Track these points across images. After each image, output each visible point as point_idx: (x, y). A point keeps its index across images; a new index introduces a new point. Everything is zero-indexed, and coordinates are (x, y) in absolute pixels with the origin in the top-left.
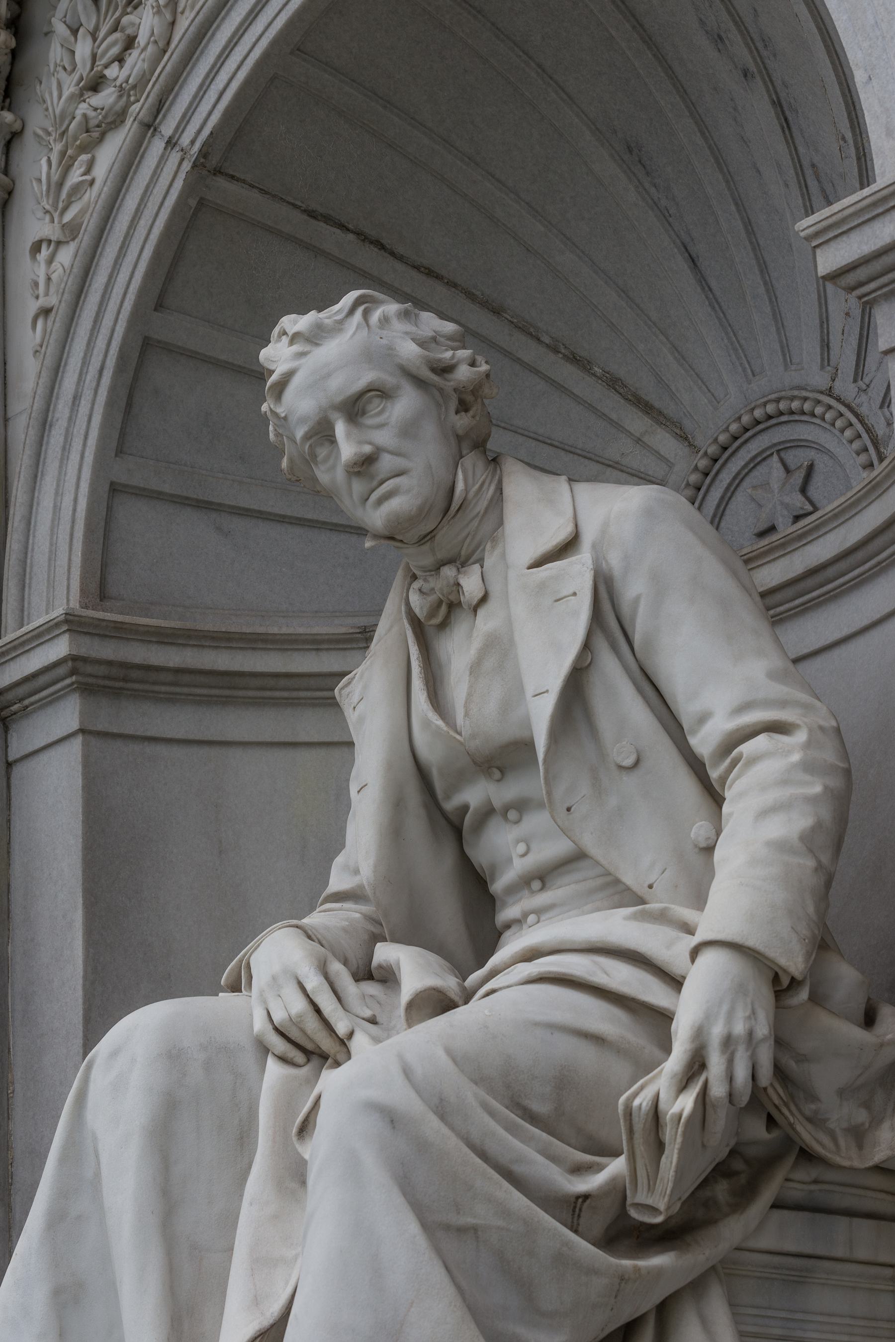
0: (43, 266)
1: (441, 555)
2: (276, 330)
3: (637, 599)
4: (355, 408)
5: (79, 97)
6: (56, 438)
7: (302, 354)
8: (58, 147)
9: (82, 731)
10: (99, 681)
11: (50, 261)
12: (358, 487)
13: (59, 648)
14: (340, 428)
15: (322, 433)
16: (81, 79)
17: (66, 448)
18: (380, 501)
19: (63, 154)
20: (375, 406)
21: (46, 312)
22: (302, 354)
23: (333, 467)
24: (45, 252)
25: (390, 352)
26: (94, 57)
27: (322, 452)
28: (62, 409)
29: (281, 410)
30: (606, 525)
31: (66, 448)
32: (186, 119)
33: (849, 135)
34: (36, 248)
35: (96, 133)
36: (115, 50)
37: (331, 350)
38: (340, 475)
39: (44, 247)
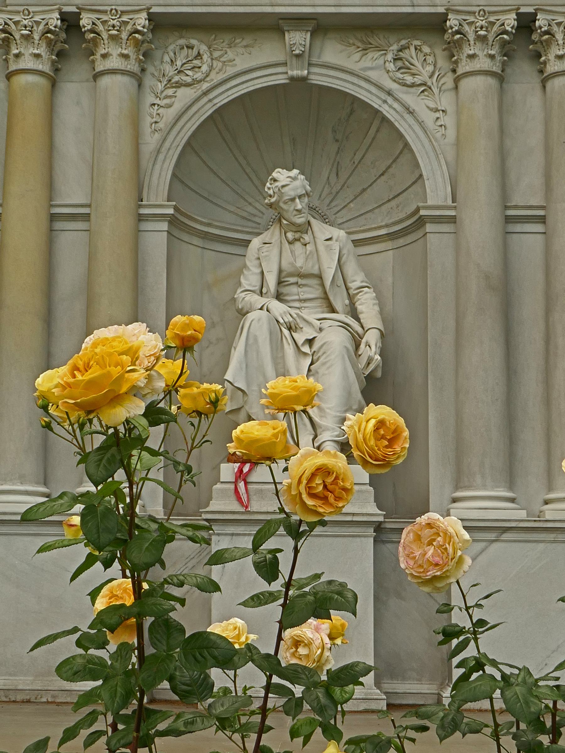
0: (155, 110)
1: (299, 230)
2: (277, 170)
3: (344, 254)
4: (300, 197)
5: (176, 75)
6: (161, 157)
7: (291, 182)
8: (165, 83)
9: (167, 231)
10: (173, 221)
11: (157, 110)
12: (295, 212)
13: (171, 211)
14: (297, 200)
15: (293, 200)
16: (177, 69)
17: (164, 160)
18: (300, 218)
19: (166, 85)
20: (303, 198)
21: (156, 122)
22: (291, 182)
23: (290, 207)
24: (156, 107)
25: (304, 187)
26: (182, 66)
27: (290, 203)
28: (164, 150)
29: (283, 191)
30: (338, 237)
31: (164, 160)
32: (216, 97)
33: (356, 163)
34: (154, 104)
35: (179, 85)
36: (189, 68)
37: (297, 183)
38: (292, 208)
39: (156, 106)
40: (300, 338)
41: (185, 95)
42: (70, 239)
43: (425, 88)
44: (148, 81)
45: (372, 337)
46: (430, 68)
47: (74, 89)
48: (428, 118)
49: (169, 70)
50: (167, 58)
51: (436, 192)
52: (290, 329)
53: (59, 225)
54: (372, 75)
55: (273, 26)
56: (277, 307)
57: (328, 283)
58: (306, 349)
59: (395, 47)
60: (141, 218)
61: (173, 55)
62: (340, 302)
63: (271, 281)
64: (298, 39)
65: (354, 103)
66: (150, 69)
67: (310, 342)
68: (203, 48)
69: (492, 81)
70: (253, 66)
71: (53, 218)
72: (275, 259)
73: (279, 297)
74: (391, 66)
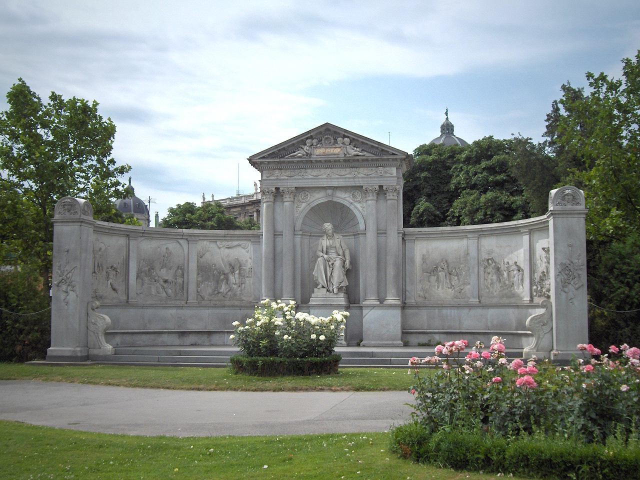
15: (329, 231)
35: (303, 202)
40: (330, 264)
41: (304, 205)
42: (278, 239)
43: (360, 202)
44: (296, 201)
45: (347, 262)
46: (360, 197)
47: (278, 204)
48: (360, 209)
49: (301, 199)
50: (300, 196)
51: (362, 226)
52: (328, 261)
53: (276, 237)
54: (348, 199)
55: (325, 188)
56: (325, 256)
57: (337, 249)
58: (331, 266)
59: (352, 192)
60: (295, 235)
61: (301, 196)
62: (341, 252)
63: (325, 249)
64: (330, 192)
65: (343, 206)
66: (296, 198)
67: (333, 264)
68: (308, 193)
69: (375, 202)
70: (318, 198)
71: (275, 235)
72: (326, 243)
73: (326, 254)
74: (352, 197)
